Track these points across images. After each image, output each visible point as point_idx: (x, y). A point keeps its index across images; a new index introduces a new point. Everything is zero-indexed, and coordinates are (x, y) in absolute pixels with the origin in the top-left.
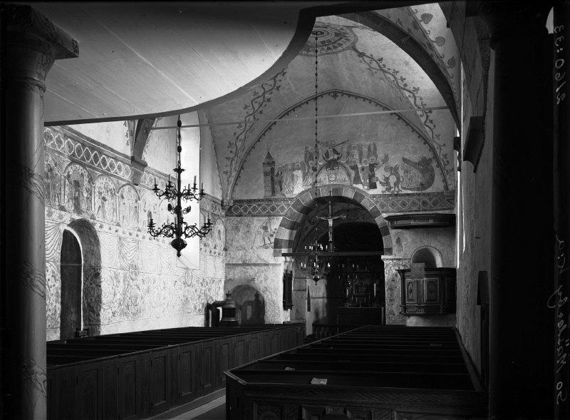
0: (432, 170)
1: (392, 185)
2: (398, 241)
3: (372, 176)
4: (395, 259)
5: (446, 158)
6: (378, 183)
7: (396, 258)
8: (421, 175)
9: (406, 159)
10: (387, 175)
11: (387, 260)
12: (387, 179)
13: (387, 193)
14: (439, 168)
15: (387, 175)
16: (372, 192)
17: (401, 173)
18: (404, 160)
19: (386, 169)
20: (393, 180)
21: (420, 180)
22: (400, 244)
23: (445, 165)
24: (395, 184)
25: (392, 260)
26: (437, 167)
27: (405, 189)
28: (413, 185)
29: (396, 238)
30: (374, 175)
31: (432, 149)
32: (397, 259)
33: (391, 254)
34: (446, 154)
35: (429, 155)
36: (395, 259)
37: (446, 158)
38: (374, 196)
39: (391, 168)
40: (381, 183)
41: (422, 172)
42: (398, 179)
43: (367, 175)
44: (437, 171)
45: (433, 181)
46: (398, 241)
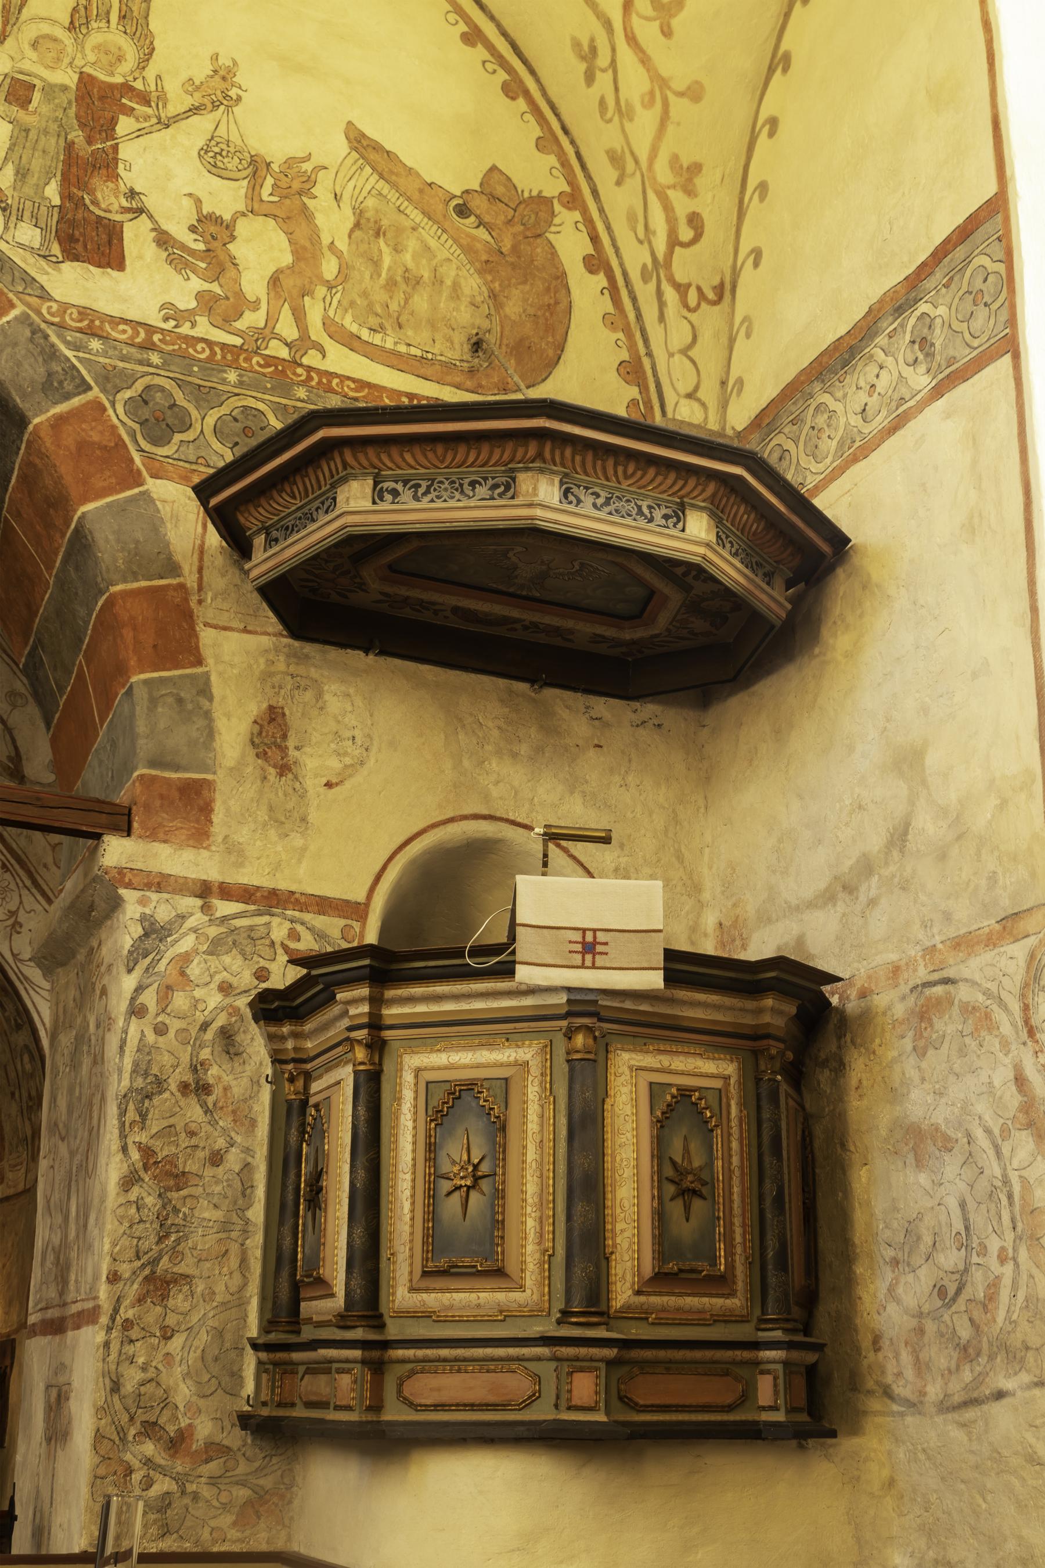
0: (560, 279)
1: (254, 283)
2: (272, 737)
3: (88, 164)
4: (226, 892)
5: (690, 191)
6: (136, 237)
7: (248, 876)
8: (472, 284)
9: (377, 147)
10: (226, 198)
11: (160, 883)
12: (215, 229)
13: (203, 328)
14: (601, 280)
15: (226, 198)
16: (73, 284)
17: (333, 223)
18: (361, 144)
19: (214, 157)
20: (260, 252)
21: (465, 317)
22: (284, 769)
23: (674, 242)
24: (275, 281)
25: (204, 891)
26: (595, 263)
27: (351, 342)
28: (417, 341)
29: (254, 708)
30: (107, 164)
31: (555, 135)
32: (246, 894)
33: (200, 836)
34: (696, 168)
35: (536, 175)
36: (226, 892)
37: (690, 191)
38: (92, 324)
39: (257, 167)
40: (163, 239)
41: (487, 266)
42: (306, 251)
43: (53, 144)
44: (587, 293)
45: (561, 347)
46: (272, 737)
